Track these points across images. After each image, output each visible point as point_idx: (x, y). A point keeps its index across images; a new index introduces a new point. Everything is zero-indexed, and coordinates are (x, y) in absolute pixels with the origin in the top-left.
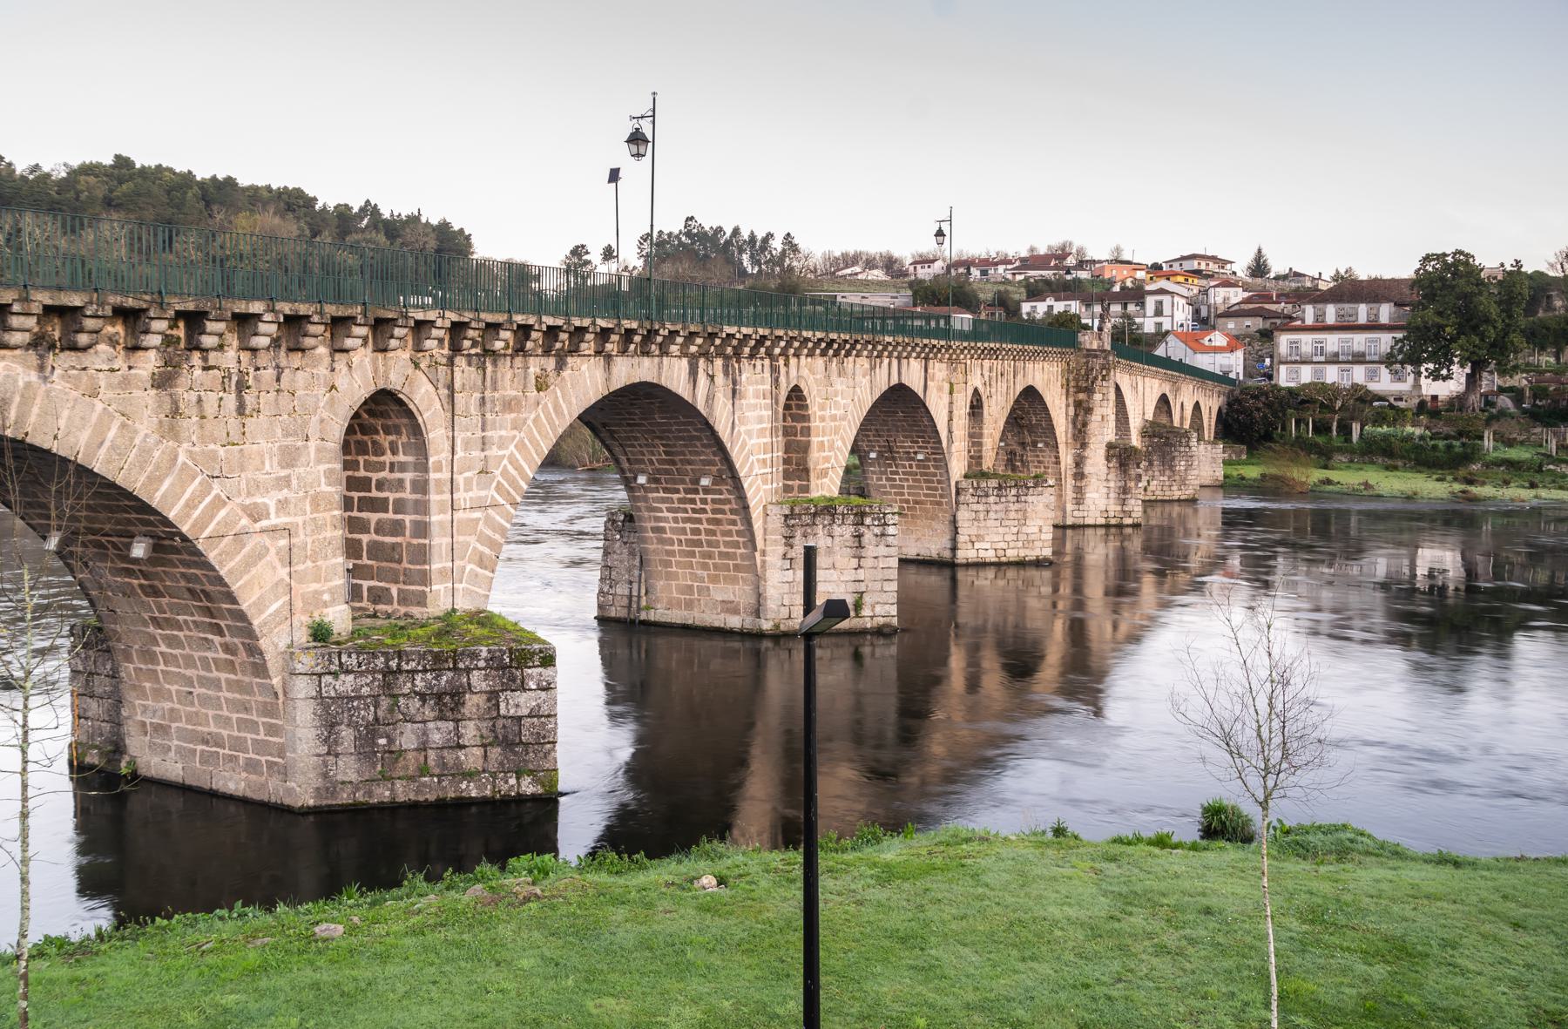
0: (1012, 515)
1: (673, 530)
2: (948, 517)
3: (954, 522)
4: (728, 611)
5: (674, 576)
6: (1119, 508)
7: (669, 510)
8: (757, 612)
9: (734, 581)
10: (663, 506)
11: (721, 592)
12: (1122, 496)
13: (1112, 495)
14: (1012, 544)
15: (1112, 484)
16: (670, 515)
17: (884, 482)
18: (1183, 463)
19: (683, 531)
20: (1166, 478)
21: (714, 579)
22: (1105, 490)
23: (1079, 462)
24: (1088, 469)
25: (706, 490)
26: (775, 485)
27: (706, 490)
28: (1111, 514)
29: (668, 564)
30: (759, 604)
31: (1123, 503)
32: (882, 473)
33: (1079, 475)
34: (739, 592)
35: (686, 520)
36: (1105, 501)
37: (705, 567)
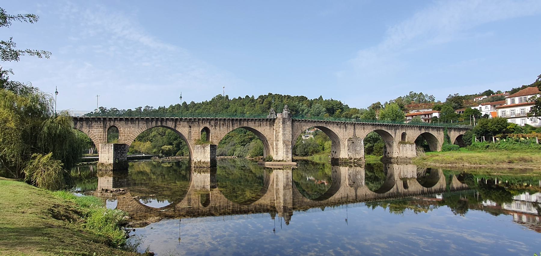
0: (203, 152)
6: (286, 156)
12: (287, 153)
13: (285, 153)
14: (203, 158)
15: (284, 150)
18: (359, 148)
20: (354, 152)
22: (283, 152)
23: (276, 145)
24: (279, 146)
26: (104, 141)
28: (284, 157)
31: (287, 155)
33: (277, 148)
36: (283, 154)
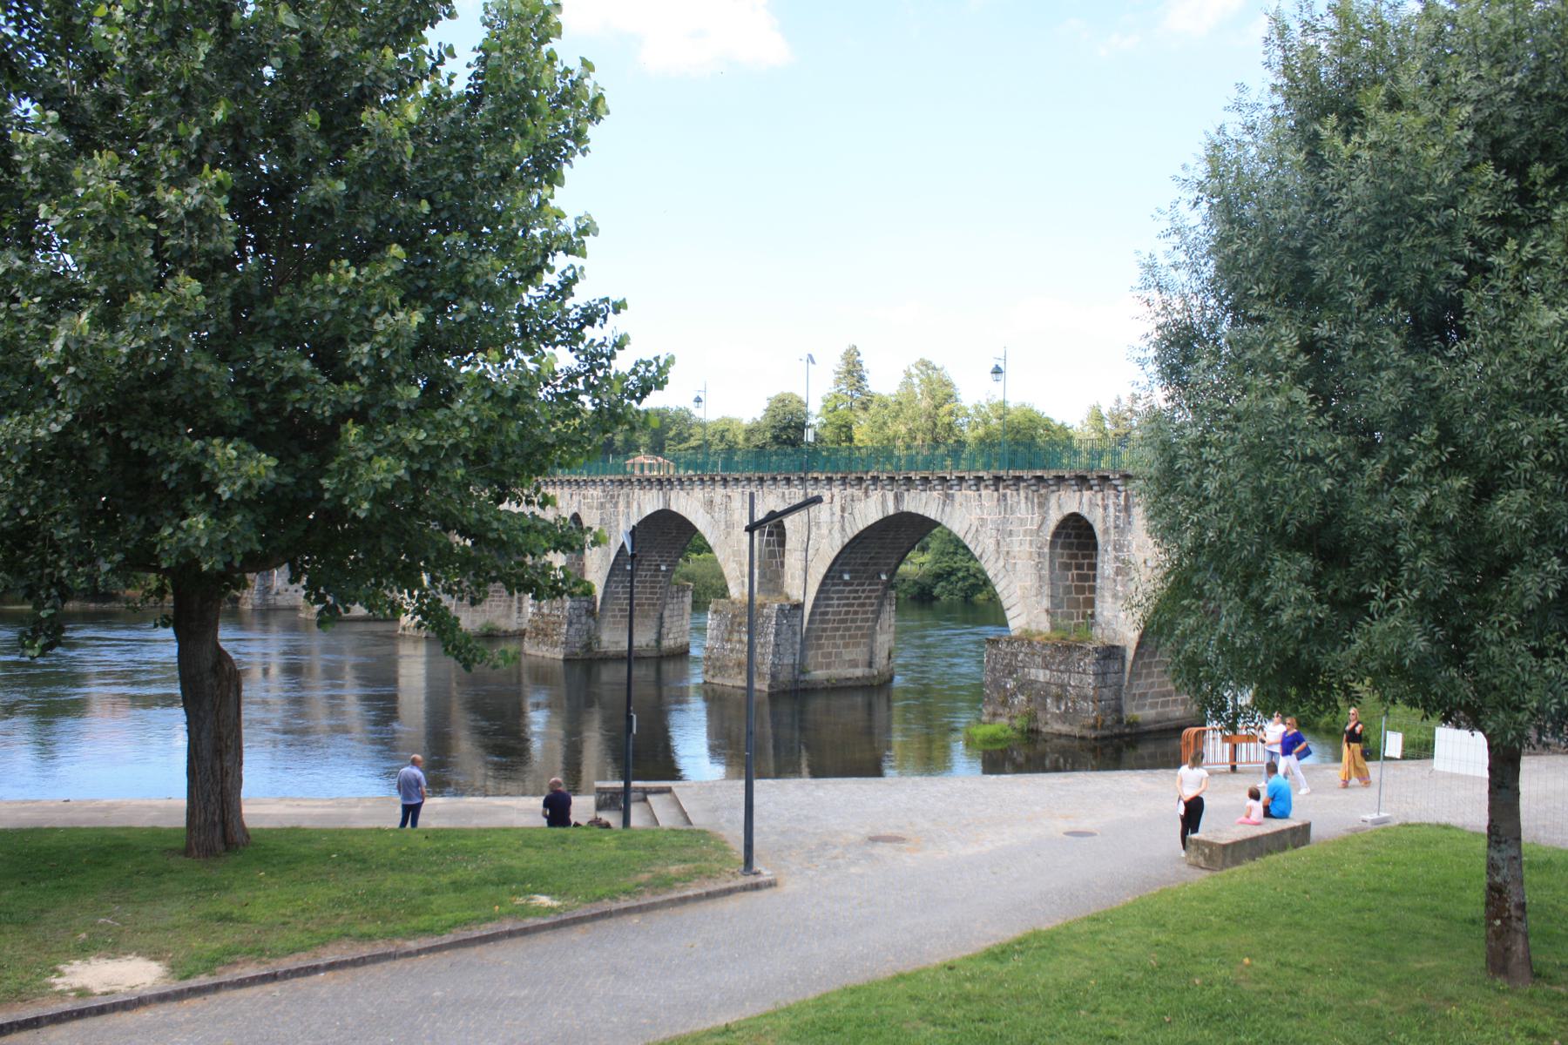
1: (834, 613)
2: (658, 614)
3: (661, 617)
4: (850, 667)
5: (820, 647)
7: (838, 599)
8: (870, 664)
9: (857, 645)
10: (835, 596)
11: (848, 654)
16: (836, 602)
17: (620, 589)
19: (840, 613)
21: (846, 646)
25: (846, 584)
27: (846, 584)
29: (819, 638)
30: (871, 658)
32: (622, 582)
34: (859, 653)
35: (845, 605)
37: (843, 637)
